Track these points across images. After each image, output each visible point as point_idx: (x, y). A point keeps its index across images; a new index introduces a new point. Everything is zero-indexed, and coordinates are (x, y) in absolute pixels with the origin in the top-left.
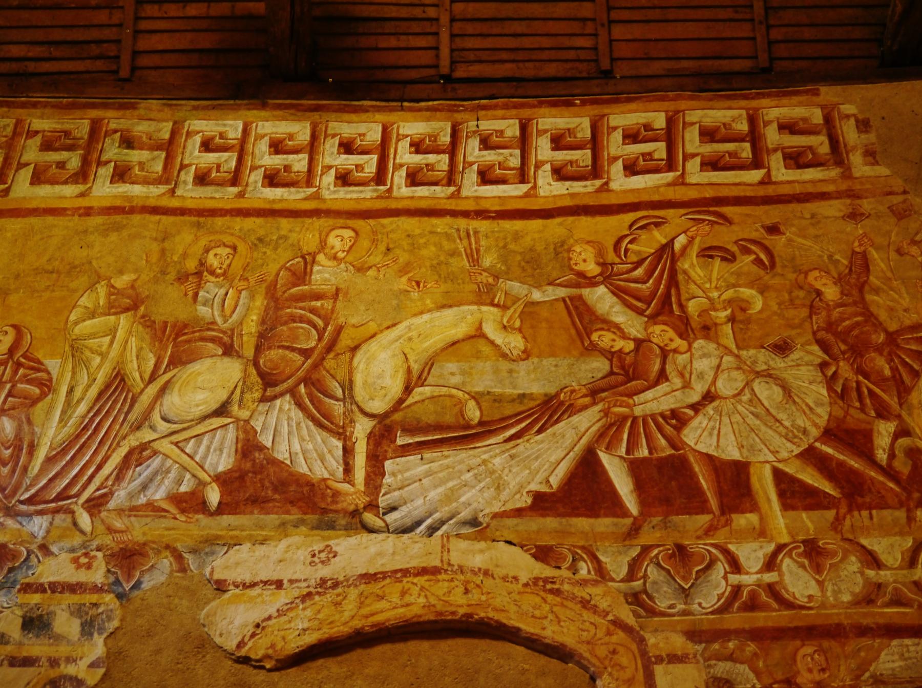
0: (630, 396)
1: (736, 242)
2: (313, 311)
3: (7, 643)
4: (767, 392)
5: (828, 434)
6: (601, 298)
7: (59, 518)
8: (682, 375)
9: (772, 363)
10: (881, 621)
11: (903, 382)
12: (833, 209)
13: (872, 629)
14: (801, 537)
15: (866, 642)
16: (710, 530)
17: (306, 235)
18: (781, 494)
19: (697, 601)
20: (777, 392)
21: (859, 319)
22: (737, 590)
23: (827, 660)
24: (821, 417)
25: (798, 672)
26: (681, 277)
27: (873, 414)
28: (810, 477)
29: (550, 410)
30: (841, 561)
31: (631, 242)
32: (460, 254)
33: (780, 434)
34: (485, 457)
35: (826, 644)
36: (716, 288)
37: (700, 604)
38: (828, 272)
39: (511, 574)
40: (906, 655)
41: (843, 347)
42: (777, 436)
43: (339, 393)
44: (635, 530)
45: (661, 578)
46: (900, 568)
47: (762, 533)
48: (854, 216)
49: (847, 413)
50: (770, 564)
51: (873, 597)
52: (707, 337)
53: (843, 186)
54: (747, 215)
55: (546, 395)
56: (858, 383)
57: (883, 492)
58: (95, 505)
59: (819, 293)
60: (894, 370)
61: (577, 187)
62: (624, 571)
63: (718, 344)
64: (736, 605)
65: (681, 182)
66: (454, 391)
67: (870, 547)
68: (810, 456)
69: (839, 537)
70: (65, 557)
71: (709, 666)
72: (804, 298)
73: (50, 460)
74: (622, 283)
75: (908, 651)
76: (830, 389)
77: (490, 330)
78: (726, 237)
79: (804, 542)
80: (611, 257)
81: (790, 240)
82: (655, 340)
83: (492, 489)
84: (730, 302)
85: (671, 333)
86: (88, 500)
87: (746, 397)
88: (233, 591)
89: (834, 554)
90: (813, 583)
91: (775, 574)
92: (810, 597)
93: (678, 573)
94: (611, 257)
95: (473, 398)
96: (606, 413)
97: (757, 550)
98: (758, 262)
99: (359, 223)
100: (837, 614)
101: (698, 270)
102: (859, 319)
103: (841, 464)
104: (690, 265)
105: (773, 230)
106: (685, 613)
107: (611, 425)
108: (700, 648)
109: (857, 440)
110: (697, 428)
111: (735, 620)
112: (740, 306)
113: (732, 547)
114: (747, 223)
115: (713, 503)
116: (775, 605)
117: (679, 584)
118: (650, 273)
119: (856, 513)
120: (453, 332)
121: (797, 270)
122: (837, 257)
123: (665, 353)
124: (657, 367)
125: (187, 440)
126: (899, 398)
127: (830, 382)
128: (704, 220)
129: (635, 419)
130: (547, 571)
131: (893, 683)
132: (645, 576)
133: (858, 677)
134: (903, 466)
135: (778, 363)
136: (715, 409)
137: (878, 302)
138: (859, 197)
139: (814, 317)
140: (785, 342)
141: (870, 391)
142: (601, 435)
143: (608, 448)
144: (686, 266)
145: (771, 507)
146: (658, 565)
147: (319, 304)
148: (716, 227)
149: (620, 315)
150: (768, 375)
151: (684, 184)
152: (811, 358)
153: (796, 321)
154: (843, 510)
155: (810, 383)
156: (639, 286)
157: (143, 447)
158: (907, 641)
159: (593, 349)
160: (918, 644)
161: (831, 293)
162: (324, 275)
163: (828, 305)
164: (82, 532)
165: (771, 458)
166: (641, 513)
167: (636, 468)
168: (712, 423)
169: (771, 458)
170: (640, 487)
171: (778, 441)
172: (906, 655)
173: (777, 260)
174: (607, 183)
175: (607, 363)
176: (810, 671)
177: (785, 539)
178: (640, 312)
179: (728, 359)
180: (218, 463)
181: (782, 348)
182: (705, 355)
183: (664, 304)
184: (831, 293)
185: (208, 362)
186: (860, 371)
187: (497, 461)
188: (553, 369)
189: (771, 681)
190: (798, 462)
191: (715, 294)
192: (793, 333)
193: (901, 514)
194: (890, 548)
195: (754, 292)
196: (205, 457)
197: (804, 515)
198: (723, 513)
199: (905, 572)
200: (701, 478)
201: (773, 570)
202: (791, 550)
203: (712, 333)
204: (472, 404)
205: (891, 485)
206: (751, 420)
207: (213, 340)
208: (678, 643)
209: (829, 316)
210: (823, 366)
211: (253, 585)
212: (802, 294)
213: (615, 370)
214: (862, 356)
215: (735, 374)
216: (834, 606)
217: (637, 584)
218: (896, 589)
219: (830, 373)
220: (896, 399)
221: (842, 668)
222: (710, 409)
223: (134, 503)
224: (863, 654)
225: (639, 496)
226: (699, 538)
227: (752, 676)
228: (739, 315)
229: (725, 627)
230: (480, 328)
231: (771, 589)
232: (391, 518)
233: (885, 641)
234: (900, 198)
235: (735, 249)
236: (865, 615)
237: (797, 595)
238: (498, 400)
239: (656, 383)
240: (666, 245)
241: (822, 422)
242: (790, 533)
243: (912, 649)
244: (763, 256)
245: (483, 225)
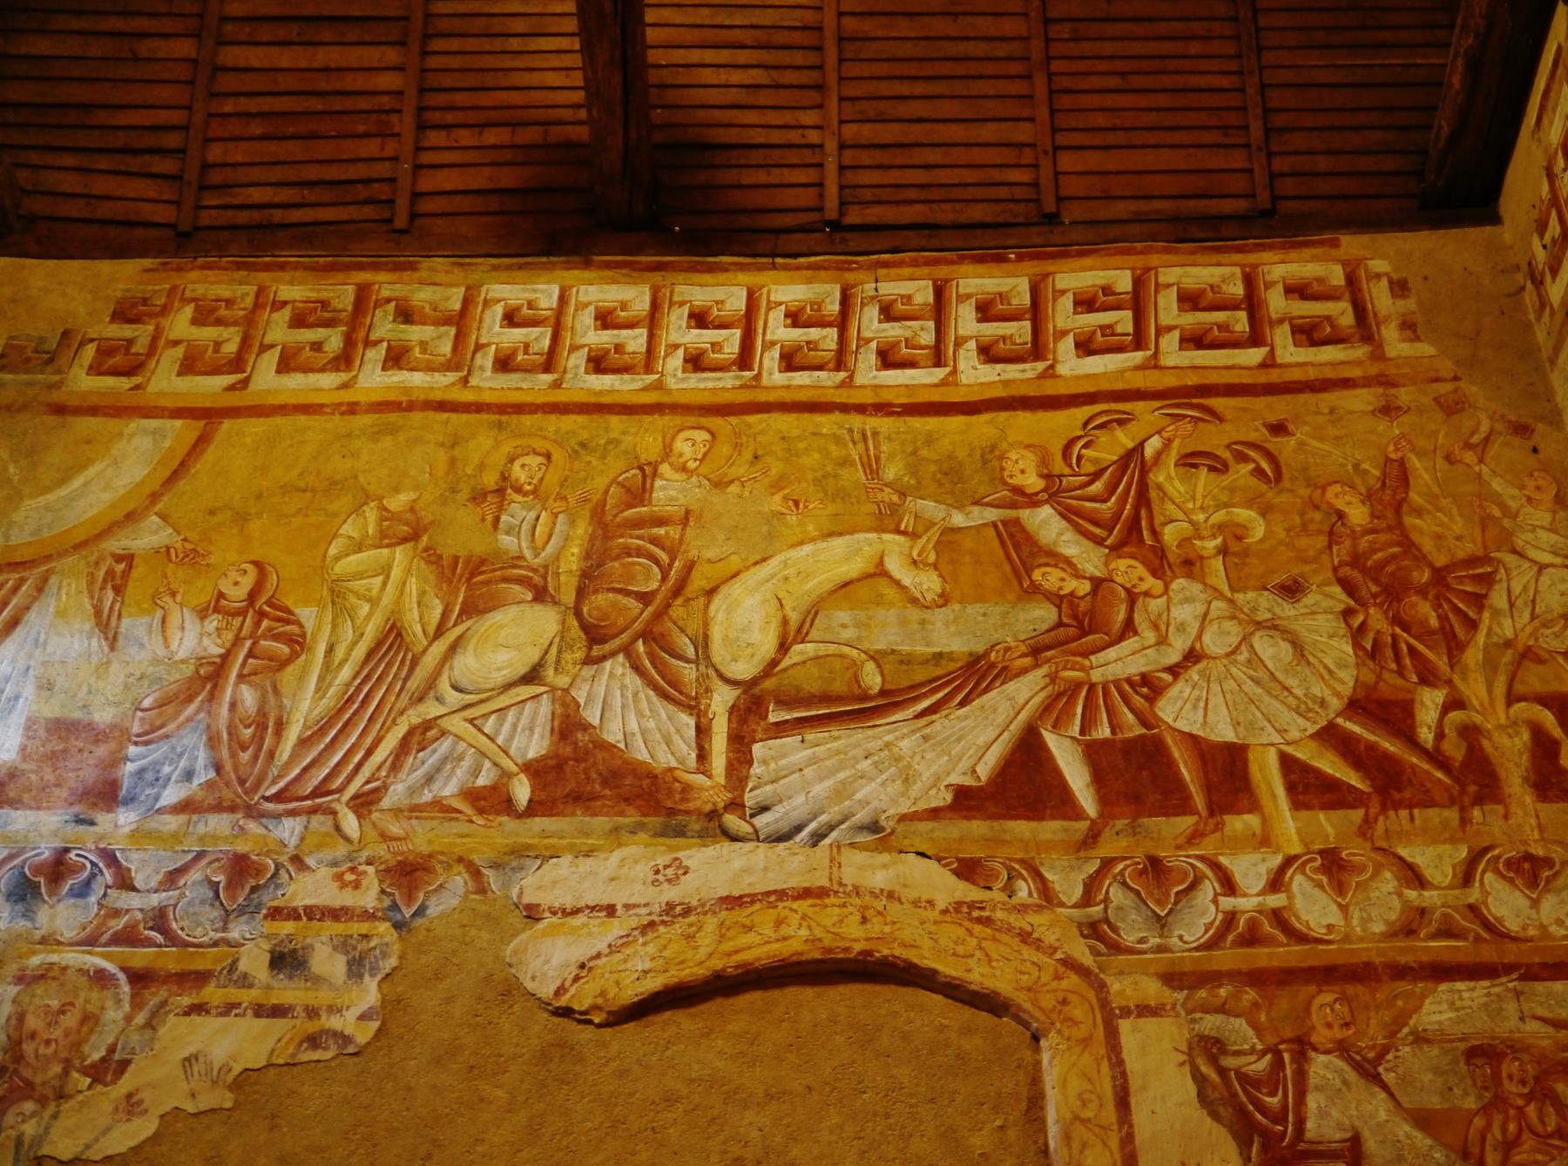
0: (1086, 654)
1: (1228, 446)
2: (654, 541)
3: (251, 986)
4: (1270, 650)
5: (1354, 707)
6: (1044, 522)
7: (317, 820)
8: (1156, 627)
9: (1278, 610)
10: (1425, 958)
11: (1455, 636)
12: (1360, 401)
13: (1412, 969)
14: (1317, 847)
15: (1403, 986)
16: (1195, 837)
17: (645, 438)
18: (1291, 788)
19: (1177, 933)
20: (1285, 649)
21: (1396, 550)
22: (1231, 918)
23: (1351, 1011)
24: (1344, 683)
25: (1313, 1028)
26: (1153, 494)
27: (1414, 678)
28: (1330, 765)
29: (976, 675)
30: (1372, 878)
31: (1085, 446)
32: (853, 463)
33: (1289, 707)
34: (888, 738)
35: (1350, 989)
36: (1202, 508)
37: (1181, 937)
38: (1352, 487)
39: (925, 897)
40: (1458, 1004)
41: (1374, 589)
42: (1285, 710)
43: (690, 651)
44: (1091, 838)
45: (1128, 902)
46: (1451, 887)
47: (1265, 841)
48: (1388, 410)
49: (1379, 678)
50: (1276, 883)
51: (1414, 926)
52: (1190, 575)
53: (1373, 370)
54: (1244, 410)
55: (971, 654)
56: (1394, 637)
57: (1429, 785)
58: (364, 803)
59: (1341, 515)
60: (1443, 619)
61: (1012, 371)
62: (1078, 892)
63: (1205, 584)
64: (1230, 938)
65: (1153, 364)
66: (846, 650)
67: (1410, 859)
68: (1330, 736)
69: (1369, 845)
70: (325, 872)
71: (1194, 1021)
72: (1321, 522)
73: (304, 743)
74: (1074, 502)
75: (1461, 999)
76: (1357, 645)
77: (894, 566)
78: (1214, 438)
79: (1321, 852)
80: (1059, 466)
81: (1302, 444)
82: (1119, 579)
83: (898, 782)
84: (1221, 528)
85: (1141, 570)
86: (355, 797)
87: (1243, 656)
88: (550, 920)
89: (1361, 869)
90: (1334, 908)
91: (1282, 896)
92: (1330, 927)
93: (1151, 895)
94: (1059, 466)
95: (872, 658)
96: (1053, 678)
97: (1258, 863)
98: (1259, 472)
99: (716, 422)
100: (1368, 950)
101: (1177, 483)
102: (1396, 550)
103: (1372, 747)
104: (1166, 477)
105: (1279, 429)
106: (1160, 949)
107: (1061, 694)
108: (1180, 996)
109: (1393, 714)
110: (1176, 699)
111: (1228, 958)
112: (1233, 534)
113: (1224, 860)
114: (1243, 421)
115: (1199, 800)
116: (1282, 938)
117: (1154, 912)
118: (1111, 488)
119: (1391, 813)
120: (845, 568)
121: (1309, 483)
122: (1366, 466)
123: (1132, 598)
124: (1121, 616)
125: (486, 716)
126: (1450, 657)
127: (1357, 635)
128: (1184, 416)
129: (1092, 687)
130: (974, 893)
131: (1440, 1041)
132: (1106, 900)
133: (1393, 1034)
134: (1454, 749)
135: (1286, 610)
136: (1201, 673)
137: (1421, 528)
138: (1394, 385)
139: (1335, 548)
140: (1296, 582)
141: (1412, 651)
142: (1046, 708)
143: (1056, 726)
144: (1161, 479)
145: (1276, 806)
146: (1124, 884)
147: (662, 531)
148: (1201, 425)
149: (1071, 545)
150: (1272, 626)
151: (1156, 367)
152: (1331, 603)
153: (1311, 553)
154: (1373, 811)
155: (1330, 637)
156: (1097, 505)
157: (427, 725)
158: (1460, 985)
159: (1034, 591)
160: (1473, 989)
161: (1358, 515)
162: (669, 492)
163: (1353, 531)
164: (348, 839)
165: (1277, 739)
166: (1101, 815)
167: (1094, 754)
168: (1196, 692)
169: (1277, 739)
170: (1099, 779)
171: (1286, 716)
172: (1458, 1004)
173: (1284, 470)
174: (1052, 367)
175: (1054, 610)
176: (1329, 1026)
177: (1296, 849)
178: (1099, 542)
179: (1218, 606)
180: (527, 748)
181: (1292, 590)
182: (1186, 600)
183: (1132, 530)
184: (1358, 515)
185: (513, 611)
186: (1397, 621)
187: (905, 744)
188: (981, 618)
189: (1276, 1040)
190: (1313, 745)
191: (1201, 517)
192: (1307, 569)
193: (1452, 814)
194: (1438, 860)
195: (1253, 514)
196: (510, 739)
197: (1322, 816)
198: (1212, 814)
199: (1457, 892)
200: (1182, 766)
201: (1279, 891)
202: (1304, 864)
203: (1196, 569)
204: (870, 666)
205: (1439, 775)
206: (1250, 687)
207: (520, 581)
208: (1152, 989)
209: (1355, 546)
210: (1347, 614)
211: (576, 911)
212: (1318, 516)
213: (1065, 620)
214: (1399, 601)
215: (1229, 625)
216: (1361, 939)
217: (1096, 911)
218: (1445, 915)
219: (1356, 623)
220: (1445, 659)
221: (1373, 1021)
222: (1194, 673)
223: (416, 801)
224: (1400, 1003)
225: (1098, 791)
226: (1179, 847)
227: (1251, 1033)
228: (1233, 544)
229: (1215, 968)
230: (881, 563)
231: (1277, 916)
232: (762, 821)
233: (1430, 985)
234: (1449, 387)
235: (1226, 455)
236: (1403, 950)
237: (1312, 925)
238: (906, 661)
239: (1121, 638)
240: (1134, 450)
241: (1347, 690)
242: (1302, 840)
243: (1465, 995)
244: (1265, 465)
245: (884, 424)
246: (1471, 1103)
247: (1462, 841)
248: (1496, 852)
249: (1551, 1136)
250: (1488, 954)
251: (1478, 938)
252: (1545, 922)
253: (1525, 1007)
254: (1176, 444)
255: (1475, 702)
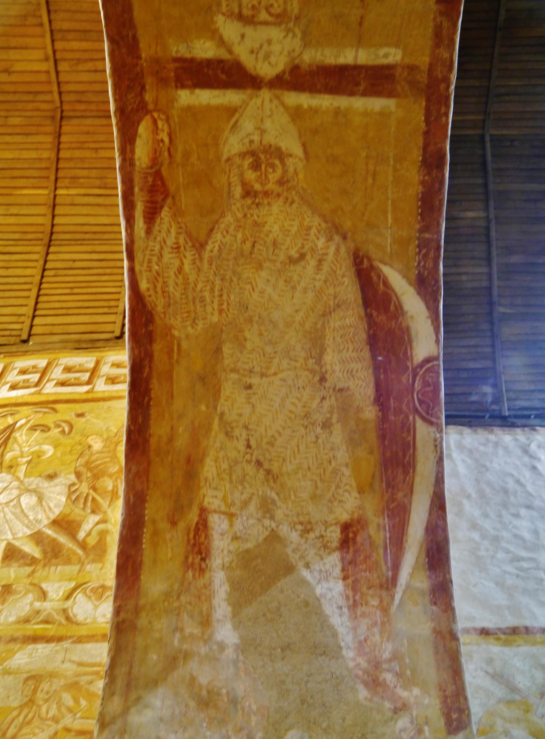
1: (55, 422)
4: (27, 501)
5: (56, 523)
9: (41, 485)
15: (11, 646)
24: (54, 513)
26: (11, 440)
27: (89, 511)
30: (21, 597)
33: (24, 524)
36: (29, 446)
41: (89, 474)
42: (21, 525)
46: (59, 600)
52: (9, 473)
60: (115, 487)
76: (69, 497)
81: (87, 421)
84: (33, 453)
105: (81, 415)
112: (39, 455)
114: (66, 412)
119: (47, 568)
134: (92, 541)
141: (94, 499)
148: (47, 415)
153: (68, 462)
155: (58, 494)
163: (92, 453)
165: (10, 537)
169: (10, 537)
172: (34, 655)
173: (74, 431)
179: (16, 483)
181: (51, 477)
193: (77, 568)
199: (61, 603)
203: (13, 470)
206: (10, 516)
209: (89, 458)
210: (74, 484)
212: (79, 447)
220: (108, 503)
235: (52, 425)
240: (13, 424)
241: (52, 517)
244: (67, 429)
246: (16, 704)
247: (75, 579)
248: (89, 584)
249: (49, 719)
250: (62, 632)
251: (60, 624)
252: (97, 615)
253: (67, 656)
254: (31, 422)
255: (113, 521)
